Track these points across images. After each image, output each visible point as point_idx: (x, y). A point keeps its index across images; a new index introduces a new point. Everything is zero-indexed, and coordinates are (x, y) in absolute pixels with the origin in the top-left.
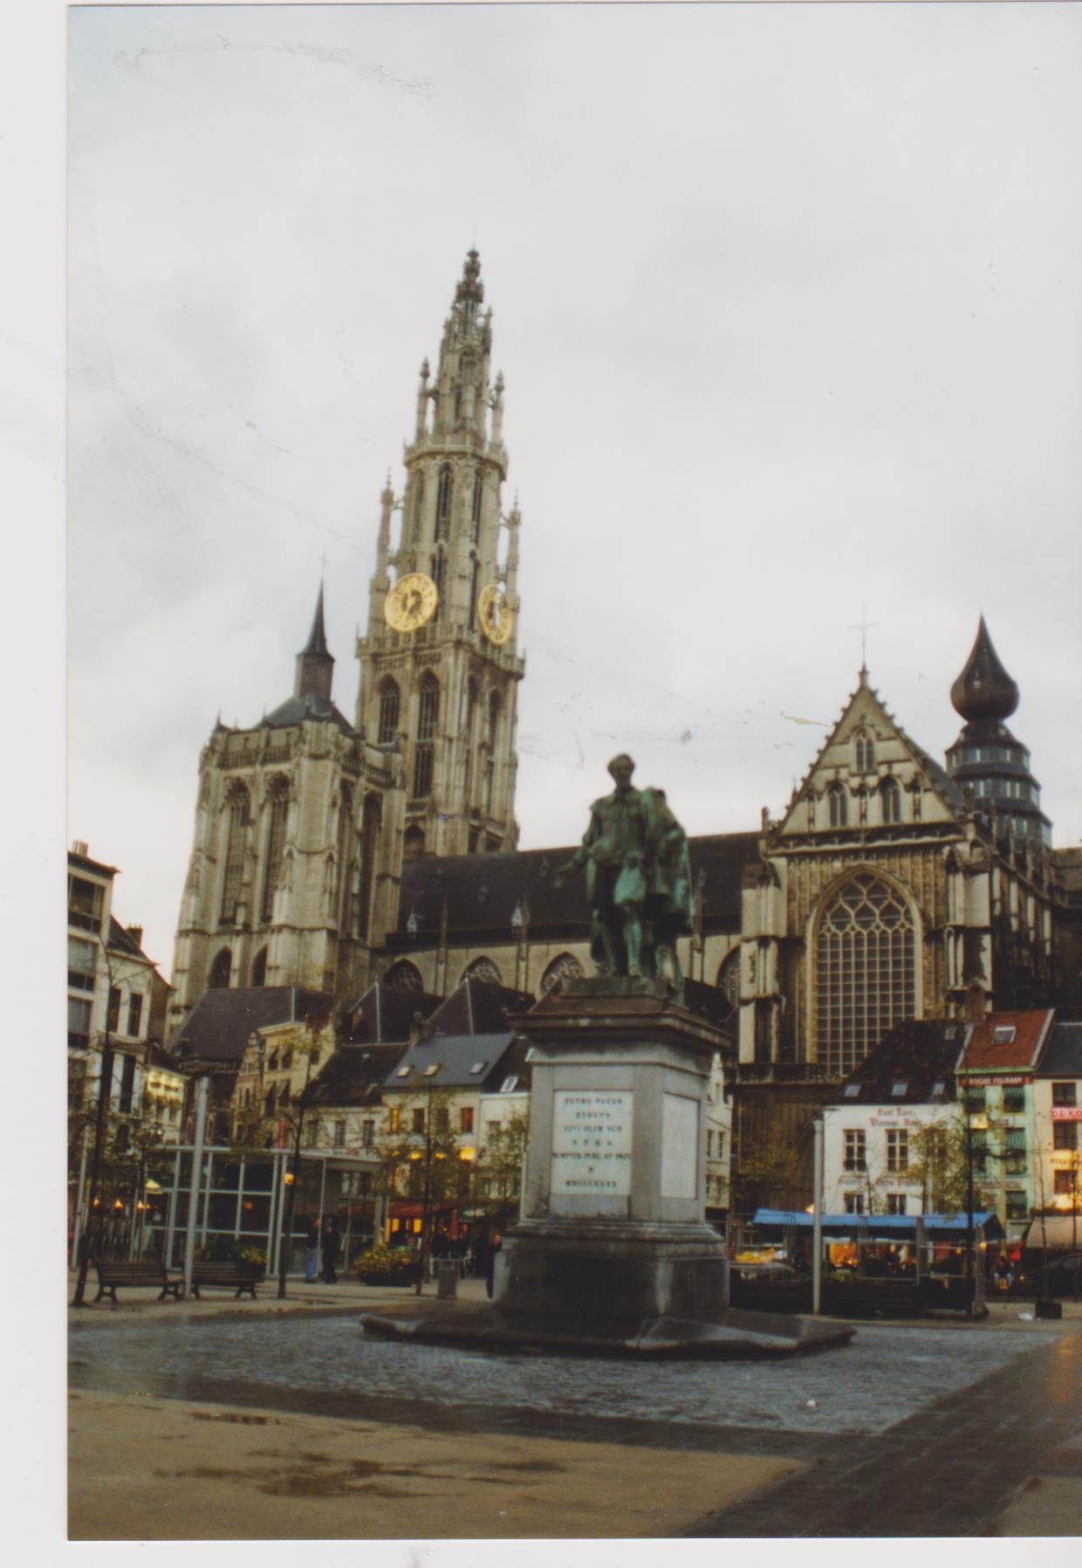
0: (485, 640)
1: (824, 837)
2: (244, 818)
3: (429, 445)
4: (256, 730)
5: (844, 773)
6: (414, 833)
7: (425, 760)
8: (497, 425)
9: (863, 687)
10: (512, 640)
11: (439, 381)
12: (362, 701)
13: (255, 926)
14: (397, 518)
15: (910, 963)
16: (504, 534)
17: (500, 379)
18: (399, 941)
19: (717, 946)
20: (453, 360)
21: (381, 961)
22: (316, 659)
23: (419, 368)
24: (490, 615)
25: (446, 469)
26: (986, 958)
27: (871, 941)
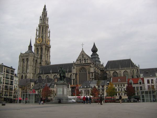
0: (47, 44)
1: (79, 64)
2: (24, 62)
3: (41, 25)
4: (25, 54)
5: (81, 58)
6: (40, 63)
7: (41, 56)
8: (48, 23)
9: (82, 51)
10: (50, 44)
11: (42, 18)
12: (35, 50)
13: (25, 73)
14: (38, 32)
15: (87, 75)
16: (49, 33)
17: (48, 18)
18: (40, 74)
19: (70, 74)
20: (43, 16)
21: (38, 76)
22: (30, 47)
23: (40, 17)
24: (47, 42)
25: (43, 27)
26: (94, 75)
27: (84, 74)
